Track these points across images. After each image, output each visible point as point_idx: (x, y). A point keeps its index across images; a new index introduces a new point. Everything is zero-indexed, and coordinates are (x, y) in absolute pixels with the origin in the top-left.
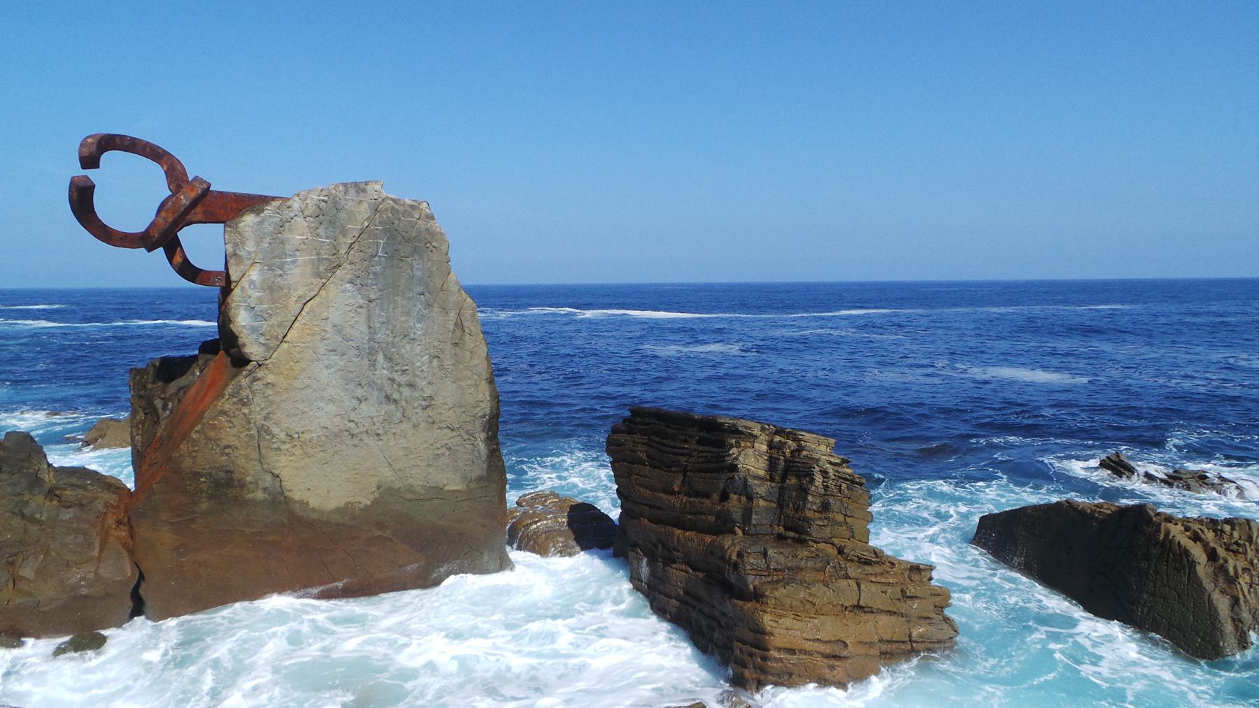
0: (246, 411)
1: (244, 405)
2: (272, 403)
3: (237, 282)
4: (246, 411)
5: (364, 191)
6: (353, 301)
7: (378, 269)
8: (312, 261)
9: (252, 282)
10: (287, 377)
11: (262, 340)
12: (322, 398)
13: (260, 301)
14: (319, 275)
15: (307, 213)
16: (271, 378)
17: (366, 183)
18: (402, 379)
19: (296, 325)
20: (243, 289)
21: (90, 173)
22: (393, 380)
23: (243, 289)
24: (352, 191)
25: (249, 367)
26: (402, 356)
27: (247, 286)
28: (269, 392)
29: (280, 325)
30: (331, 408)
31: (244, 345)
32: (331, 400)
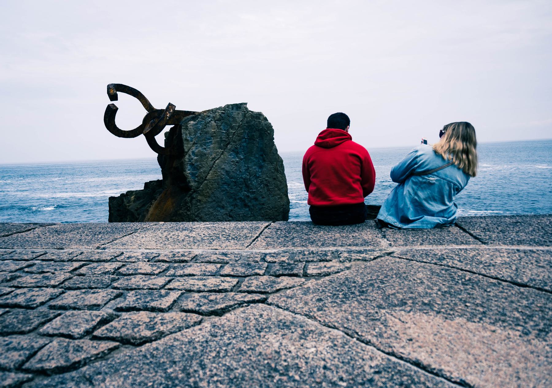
0: (189, 213)
1: (189, 210)
2: (199, 209)
3: (187, 152)
4: (189, 213)
5: (240, 108)
6: (233, 160)
7: (245, 144)
8: (217, 142)
9: (193, 152)
10: (206, 197)
11: (196, 179)
12: (219, 206)
13: (196, 161)
14: (220, 148)
15: (216, 119)
16: (199, 198)
17: (241, 104)
18: (252, 196)
19: (211, 172)
20: (190, 156)
21: (114, 102)
22: (248, 196)
23: (190, 156)
24: (235, 108)
25: (191, 193)
26: (253, 185)
27: (191, 153)
28: (199, 204)
29: (204, 172)
30: (222, 211)
31: (189, 182)
32: (223, 207)
